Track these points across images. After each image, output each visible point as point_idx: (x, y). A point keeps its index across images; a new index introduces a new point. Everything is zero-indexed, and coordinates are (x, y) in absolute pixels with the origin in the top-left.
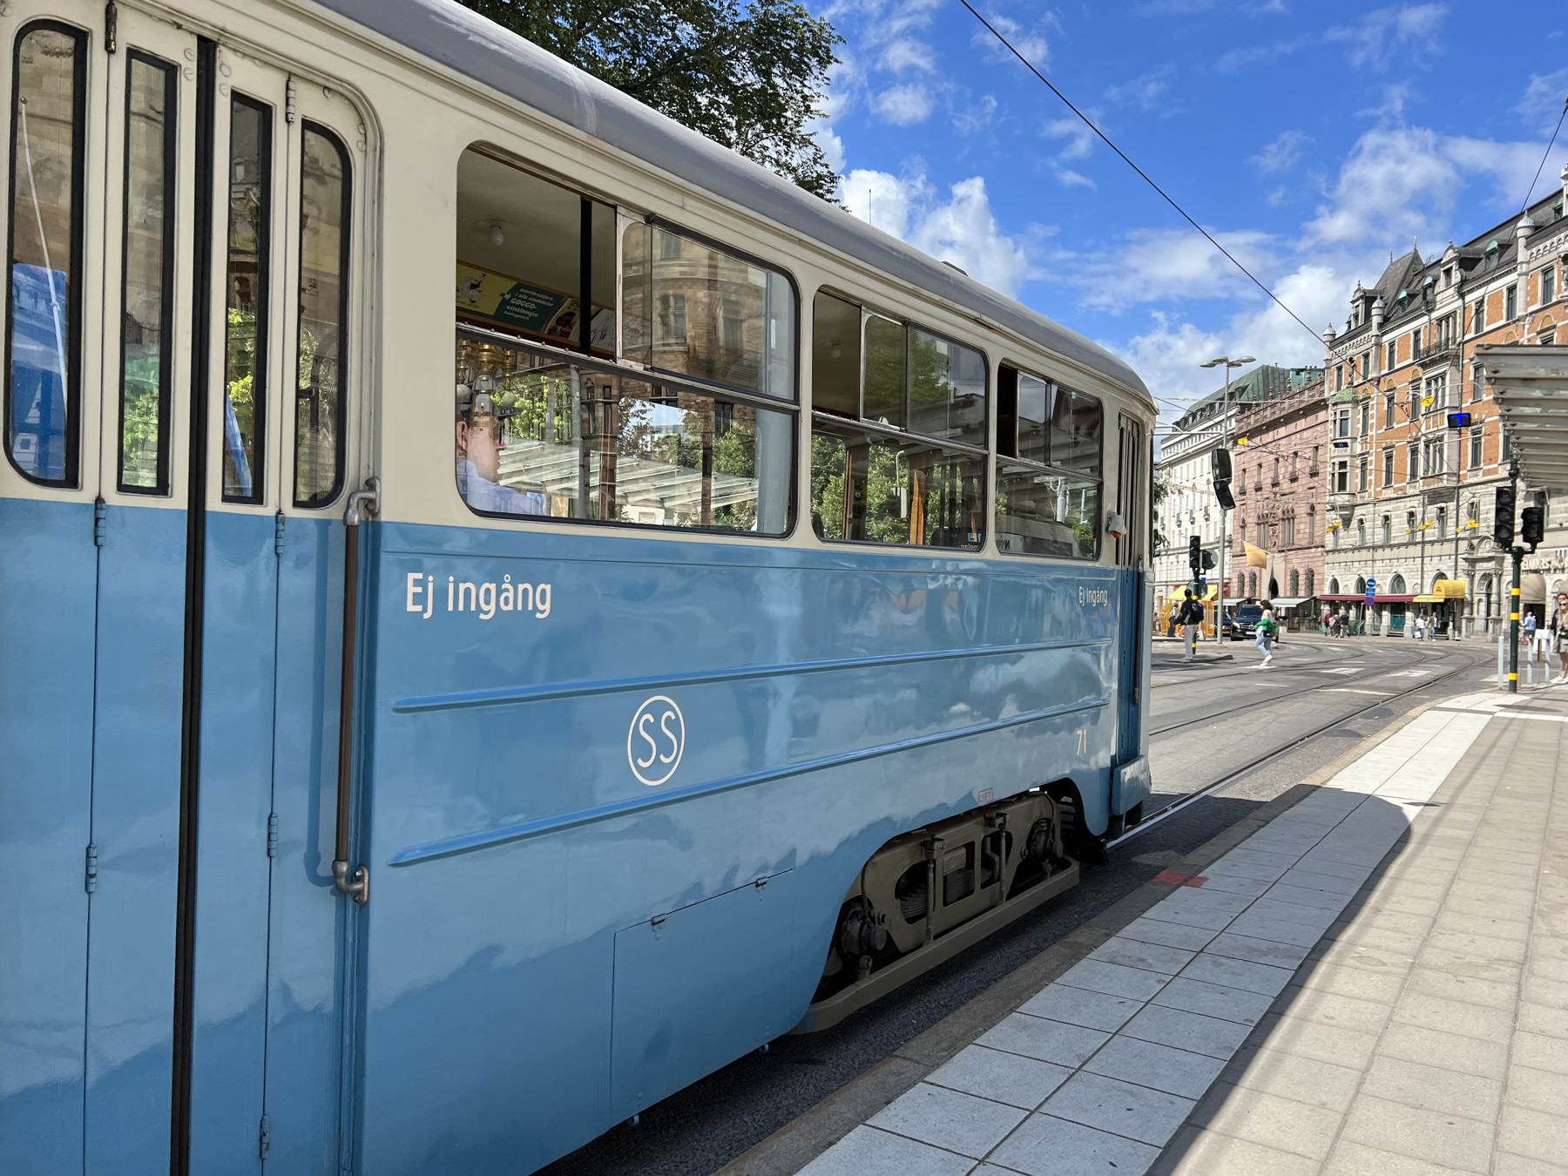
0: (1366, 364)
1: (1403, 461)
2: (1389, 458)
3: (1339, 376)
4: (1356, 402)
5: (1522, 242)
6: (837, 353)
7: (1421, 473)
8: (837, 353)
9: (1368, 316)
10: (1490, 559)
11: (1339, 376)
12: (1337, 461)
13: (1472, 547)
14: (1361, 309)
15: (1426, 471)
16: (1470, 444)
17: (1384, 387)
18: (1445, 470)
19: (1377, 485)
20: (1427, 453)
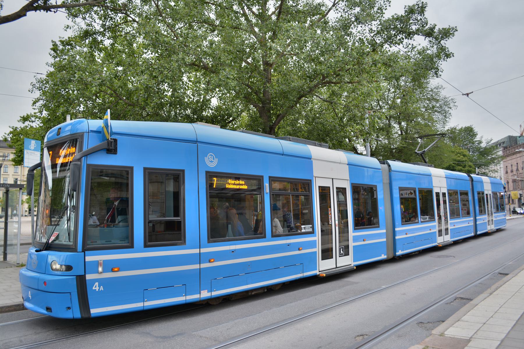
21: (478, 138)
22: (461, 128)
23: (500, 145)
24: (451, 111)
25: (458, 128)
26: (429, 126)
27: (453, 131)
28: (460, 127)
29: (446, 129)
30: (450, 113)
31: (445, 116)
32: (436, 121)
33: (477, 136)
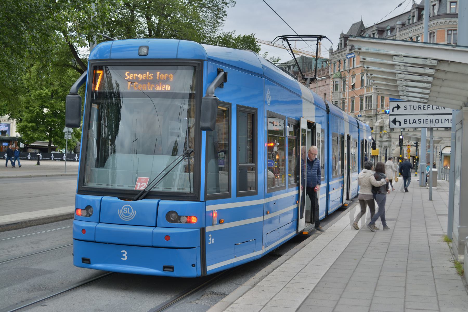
0: (345, 63)
3: (334, 66)
4: (341, 77)
6: (181, 3)
8: (181, 3)
9: (346, 45)
11: (334, 66)
12: (334, 101)
13: (381, 137)
14: (343, 42)
15: (366, 108)
16: (380, 99)
17: (351, 73)
18: (372, 108)
19: (348, 111)
20: (366, 101)
22: (239, 37)
23: (289, 67)
24: (226, 9)
25: (233, 36)
26: (192, 27)
28: (237, 36)
29: (217, 34)
30: (224, 12)
31: (217, 16)
32: (203, 21)
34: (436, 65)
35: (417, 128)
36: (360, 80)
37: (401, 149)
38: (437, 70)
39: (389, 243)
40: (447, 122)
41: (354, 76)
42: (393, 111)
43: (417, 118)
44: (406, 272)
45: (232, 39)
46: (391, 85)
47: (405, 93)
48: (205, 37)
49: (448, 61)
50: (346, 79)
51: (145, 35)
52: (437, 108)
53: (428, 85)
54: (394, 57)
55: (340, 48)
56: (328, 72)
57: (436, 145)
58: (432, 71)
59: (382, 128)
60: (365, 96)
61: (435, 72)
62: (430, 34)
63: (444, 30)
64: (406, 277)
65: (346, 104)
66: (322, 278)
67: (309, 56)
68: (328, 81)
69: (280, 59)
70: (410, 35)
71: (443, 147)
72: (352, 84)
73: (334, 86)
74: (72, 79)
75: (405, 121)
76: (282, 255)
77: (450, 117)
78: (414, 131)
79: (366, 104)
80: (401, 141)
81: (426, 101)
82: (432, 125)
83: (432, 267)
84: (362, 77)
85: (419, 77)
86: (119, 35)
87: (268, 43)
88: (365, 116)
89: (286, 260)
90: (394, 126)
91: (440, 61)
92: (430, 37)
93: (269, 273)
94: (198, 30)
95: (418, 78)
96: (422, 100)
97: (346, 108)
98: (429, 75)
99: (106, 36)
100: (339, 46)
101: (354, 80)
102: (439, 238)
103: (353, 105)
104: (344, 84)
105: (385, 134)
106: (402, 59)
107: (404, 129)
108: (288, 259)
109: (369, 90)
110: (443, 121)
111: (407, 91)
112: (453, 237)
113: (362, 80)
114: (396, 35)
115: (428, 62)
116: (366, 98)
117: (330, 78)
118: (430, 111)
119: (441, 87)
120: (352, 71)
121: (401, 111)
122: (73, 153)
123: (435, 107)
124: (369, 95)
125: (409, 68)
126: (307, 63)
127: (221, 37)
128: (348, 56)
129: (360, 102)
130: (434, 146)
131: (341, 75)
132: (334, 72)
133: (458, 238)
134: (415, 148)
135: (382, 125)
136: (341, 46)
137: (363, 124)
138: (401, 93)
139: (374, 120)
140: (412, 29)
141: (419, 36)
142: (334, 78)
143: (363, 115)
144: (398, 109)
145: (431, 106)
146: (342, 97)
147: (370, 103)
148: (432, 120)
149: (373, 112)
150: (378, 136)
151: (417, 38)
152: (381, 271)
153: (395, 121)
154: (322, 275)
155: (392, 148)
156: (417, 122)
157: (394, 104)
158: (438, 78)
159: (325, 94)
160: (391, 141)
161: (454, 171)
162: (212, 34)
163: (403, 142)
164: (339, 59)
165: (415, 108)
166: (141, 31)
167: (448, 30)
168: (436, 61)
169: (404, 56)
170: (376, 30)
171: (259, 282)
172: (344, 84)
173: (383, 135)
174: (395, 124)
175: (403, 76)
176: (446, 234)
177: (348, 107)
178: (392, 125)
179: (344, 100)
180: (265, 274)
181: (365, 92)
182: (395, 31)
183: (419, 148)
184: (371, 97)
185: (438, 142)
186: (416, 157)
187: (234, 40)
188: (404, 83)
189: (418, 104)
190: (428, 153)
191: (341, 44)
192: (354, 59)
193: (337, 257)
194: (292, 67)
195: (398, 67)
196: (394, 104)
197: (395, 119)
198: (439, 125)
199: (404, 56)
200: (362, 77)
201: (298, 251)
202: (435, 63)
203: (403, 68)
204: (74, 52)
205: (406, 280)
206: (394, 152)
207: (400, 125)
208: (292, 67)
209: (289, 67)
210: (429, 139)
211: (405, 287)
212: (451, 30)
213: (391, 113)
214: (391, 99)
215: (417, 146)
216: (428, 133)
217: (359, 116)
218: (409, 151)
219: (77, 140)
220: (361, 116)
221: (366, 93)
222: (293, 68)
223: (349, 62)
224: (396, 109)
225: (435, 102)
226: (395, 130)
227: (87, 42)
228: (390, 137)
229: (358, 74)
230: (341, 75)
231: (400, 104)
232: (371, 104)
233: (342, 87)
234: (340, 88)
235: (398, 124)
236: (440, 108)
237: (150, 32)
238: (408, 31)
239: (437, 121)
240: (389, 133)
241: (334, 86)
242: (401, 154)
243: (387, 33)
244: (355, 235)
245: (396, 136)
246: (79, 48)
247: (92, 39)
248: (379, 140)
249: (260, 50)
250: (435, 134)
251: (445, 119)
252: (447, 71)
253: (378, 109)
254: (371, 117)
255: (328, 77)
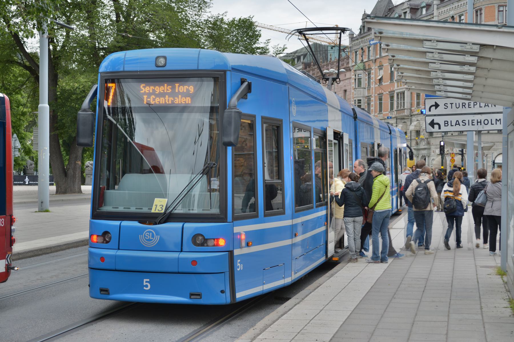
0: (369, 51)
1: (386, 101)
2: (381, 99)
3: (356, 55)
4: (365, 69)
5: (435, 7)
7: (395, 108)
10: (425, 149)
11: (356, 55)
12: (356, 99)
13: (417, 144)
15: (398, 107)
16: (415, 96)
18: (406, 107)
19: (375, 112)
20: (398, 98)
21: (261, 43)
23: (299, 58)
26: (171, 9)
27: (216, 24)
28: (231, 19)
33: (261, 40)
34: (478, 51)
35: (463, 131)
36: (390, 72)
37: (442, 158)
38: (480, 58)
39: (427, 279)
40: (498, 123)
41: (381, 67)
42: (430, 111)
43: (460, 118)
44: (448, 316)
45: (225, 23)
46: (424, 78)
47: (442, 88)
48: (188, 21)
49: (493, 46)
50: (372, 72)
51: (111, 20)
52: (485, 106)
53: (471, 77)
54: (425, 42)
55: (362, 32)
56: (348, 63)
57: (486, 152)
58: (474, 59)
59: (418, 133)
60: (396, 92)
61: (478, 60)
62: (477, 12)
63: (494, 6)
64: (448, 322)
65: (371, 103)
66: (341, 327)
67: (323, 43)
68: (348, 75)
69: (286, 48)
70: (452, 13)
71: (496, 154)
72: (379, 78)
73: (357, 80)
74: (19, 79)
75: (446, 123)
76: (290, 298)
77: (500, 116)
78: (458, 135)
79: (398, 103)
80: (442, 148)
81: (469, 97)
82: (480, 128)
83: (481, 308)
84: (391, 68)
85: (458, 67)
86: (78, 20)
87: (271, 27)
88: (397, 118)
89: (296, 305)
90: (432, 130)
91: (482, 46)
92: (477, 15)
93: (274, 322)
94: (179, 12)
95: (457, 68)
96: (464, 96)
97: (372, 108)
98: (471, 64)
99: (61, 22)
100: (361, 29)
101: (382, 73)
102: (490, 271)
103: (381, 104)
104: (369, 78)
105: (422, 139)
106: (435, 44)
107: (446, 133)
108: (298, 303)
109: (401, 84)
110: (494, 122)
111: (444, 85)
112: (508, 270)
113: (392, 73)
114: (433, 14)
115: (468, 48)
116: (398, 95)
117: (350, 70)
118: (477, 109)
119: (486, 79)
120: (378, 61)
121: (441, 110)
122: (22, 174)
123: (483, 105)
124: (401, 90)
125: (444, 55)
126: (321, 52)
127: (210, 21)
128: (372, 42)
129: (389, 100)
130: (483, 154)
131: (364, 66)
132: (356, 62)
133: (513, 270)
134: (460, 156)
135: (418, 129)
136: (364, 30)
137: (395, 128)
138: (437, 88)
139: (409, 123)
140: (454, 6)
141: (462, 15)
142: (355, 71)
143: (394, 116)
144: (436, 108)
145: (478, 103)
146: (366, 95)
147: (402, 101)
148: (479, 121)
149: (406, 113)
150: (414, 143)
151: (460, 17)
152: (416, 315)
153: (432, 124)
154: (341, 323)
155: (432, 158)
156: (461, 123)
157: (430, 102)
158: (482, 68)
159: (345, 91)
160: (430, 149)
161: (507, 185)
162: (197, 17)
163: (446, 150)
164: (362, 45)
165: (458, 107)
166: (106, 15)
167: (499, 6)
168: (479, 46)
169: (437, 41)
170: (408, 8)
171: (260, 334)
172: (369, 78)
173: (421, 141)
174: (433, 128)
175: (437, 66)
176: (499, 265)
177: (375, 107)
178: (430, 129)
179: (369, 98)
180: (268, 323)
181: (396, 88)
182: (431, 8)
183: (466, 156)
184: (404, 93)
185: (489, 148)
186: (462, 168)
187: (227, 24)
188: (439, 74)
189: (461, 102)
190: (476, 162)
191: (364, 27)
192: (380, 45)
193: (361, 299)
194: (302, 57)
195: (430, 55)
196: (430, 102)
197: (433, 120)
198: (489, 127)
199: (437, 41)
200: (391, 68)
201: (311, 293)
202: (476, 48)
203: (437, 56)
204: (20, 45)
205: (448, 326)
206: (434, 162)
207: (440, 128)
208: (302, 57)
209: (299, 58)
210: (477, 144)
211: (447, 334)
212: (503, 6)
213: (428, 113)
214: (427, 96)
215: (462, 154)
216: (475, 138)
217: (388, 118)
218: (453, 160)
219: (27, 158)
220: (391, 118)
221: (397, 88)
222: (304, 59)
223: (374, 49)
224: (434, 107)
225: (481, 98)
226: (435, 135)
227: (35, 31)
228: (428, 143)
229: (386, 64)
230: (364, 66)
231: (439, 101)
232: (404, 103)
233: (367, 82)
234: (364, 82)
235: (436, 127)
236: (490, 105)
237: (118, 16)
238: (448, 8)
239: (486, 122)
240: (427, 139)
241: (357, 80)
242: (442, 165)
243: (422, 12)
244: (383, 270)
245: (436, 143)
246: (25, 39)
247: (41, 26)
248: (415, 147)
249: (260, 37)
250: (484, 138)
251: (496, 120)
252: (493, 59)
253: (413, 109)
254: (404, 119)
255: (348, 69)
